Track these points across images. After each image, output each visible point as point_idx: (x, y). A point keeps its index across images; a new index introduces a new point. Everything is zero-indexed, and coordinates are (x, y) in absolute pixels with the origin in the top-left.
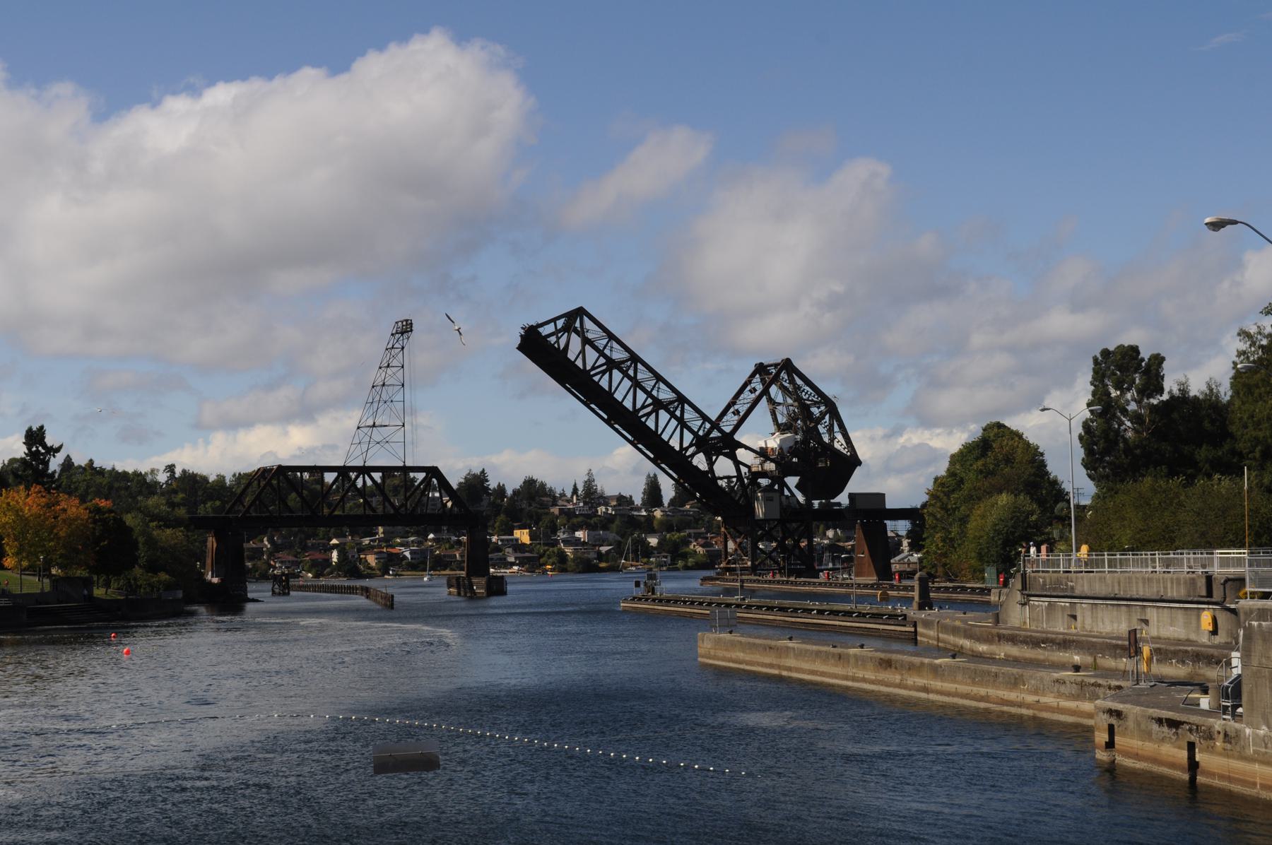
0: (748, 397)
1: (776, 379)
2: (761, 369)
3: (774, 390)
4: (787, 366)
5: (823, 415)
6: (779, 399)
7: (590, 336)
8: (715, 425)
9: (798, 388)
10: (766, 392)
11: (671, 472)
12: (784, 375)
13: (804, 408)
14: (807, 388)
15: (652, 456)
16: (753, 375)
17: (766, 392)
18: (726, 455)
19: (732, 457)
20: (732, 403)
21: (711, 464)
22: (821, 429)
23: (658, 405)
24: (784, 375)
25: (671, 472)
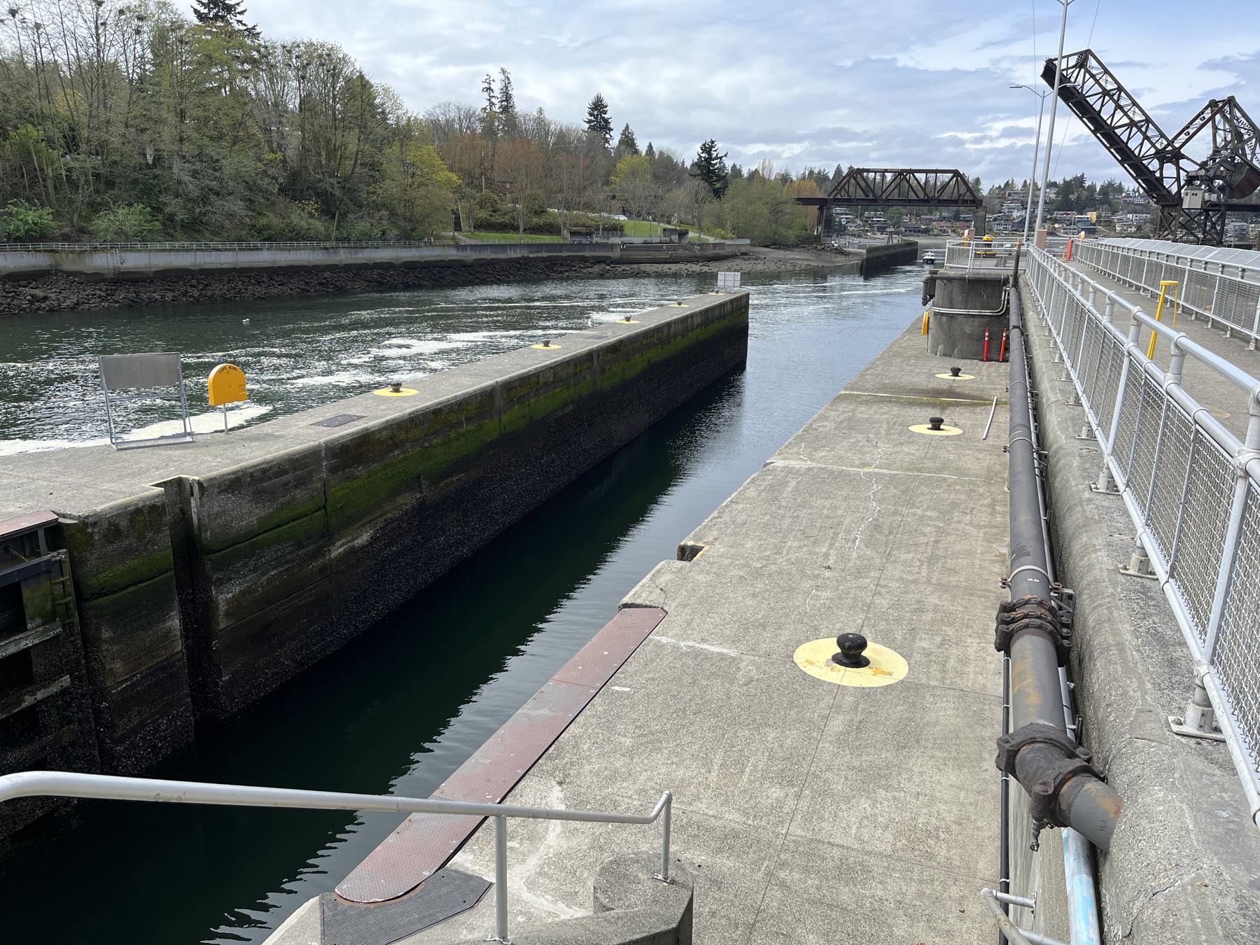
0: (1198, 122)
1: (1221, 111)
2: (1213, 104)
3: (1218, 117)
4: (1231, 101)
5: (1250, 139)
6: (1221, 126)
7: (1094, 72)
8: (1170, 143)
9: (1234, 117)
10: (1212, 118)
11: (1117, 155)
12: (1227, 108)
13: (1239, 136)
14: (1243, 120)
15: (1120, 158)
16: (1206, 108)
17: (1212, 118)
18: (1172, 163)
19: (1177, 165)
20: (1187, 127)
21: (1161, 169)
22: (1248, 151)
23: (1132, 124)
24: (1227, 108)
25: (1117, 155)
